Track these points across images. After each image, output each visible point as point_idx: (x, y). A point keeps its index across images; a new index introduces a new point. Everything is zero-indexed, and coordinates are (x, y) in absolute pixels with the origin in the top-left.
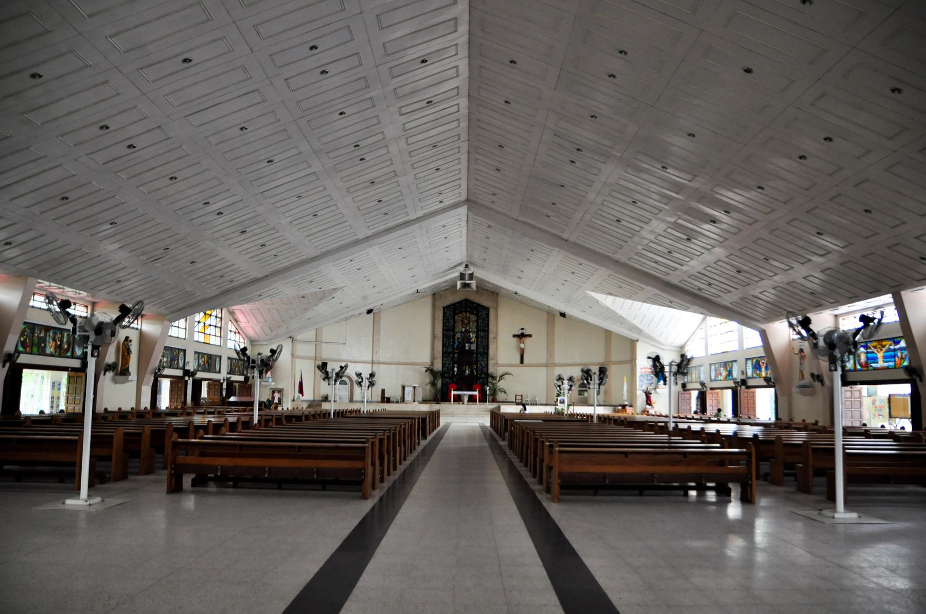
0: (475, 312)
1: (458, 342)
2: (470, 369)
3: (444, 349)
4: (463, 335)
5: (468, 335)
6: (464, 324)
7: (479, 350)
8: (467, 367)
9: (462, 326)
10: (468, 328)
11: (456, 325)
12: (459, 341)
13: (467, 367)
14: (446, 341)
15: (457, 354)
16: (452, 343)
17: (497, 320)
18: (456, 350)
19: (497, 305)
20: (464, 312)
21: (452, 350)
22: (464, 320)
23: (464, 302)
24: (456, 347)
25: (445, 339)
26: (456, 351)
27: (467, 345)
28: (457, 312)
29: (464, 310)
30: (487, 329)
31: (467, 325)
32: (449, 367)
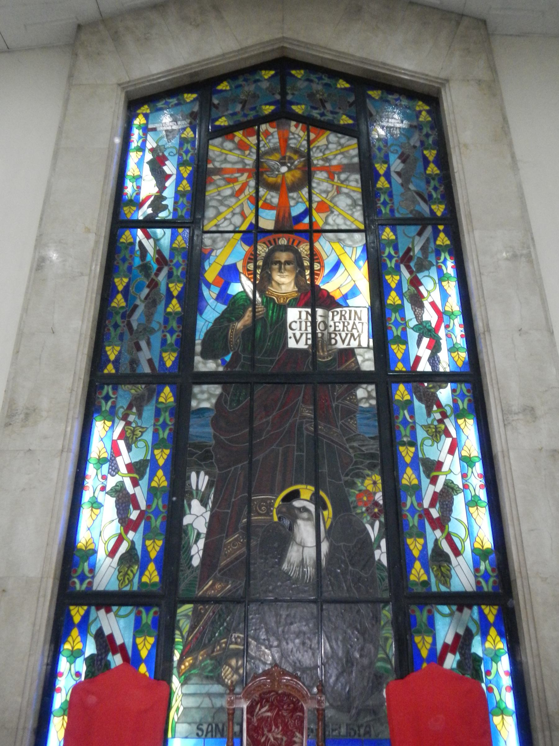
0: (345, 120)
1: (222, 296)
2: (328, 514)
3: (112, 353)
4: (262, 249)
5: (304, 249)
6: (272, 187)
7: (397, 350)
8: (306, 491)
9: (256, 199)
10: (296, 211)
11: (211, 191)
12: (235, 289)
13: (306, 491)
14: (126, 292)
15: (217, 390)
16: (175, 306)
17: (510, 145)
18: (206, 355)
19: (493, 69)
20: (268, 119)
21: (169, 359)
22: (272, 161)
23: (267, 74)
24: (210, 334)
25: (120, 283)
26: (211, 366)
27: (293, 314)
28: (222, 122)
29: (268, 109)
30: (439, 210)
31: (295, 187)
32: (141, 494)
